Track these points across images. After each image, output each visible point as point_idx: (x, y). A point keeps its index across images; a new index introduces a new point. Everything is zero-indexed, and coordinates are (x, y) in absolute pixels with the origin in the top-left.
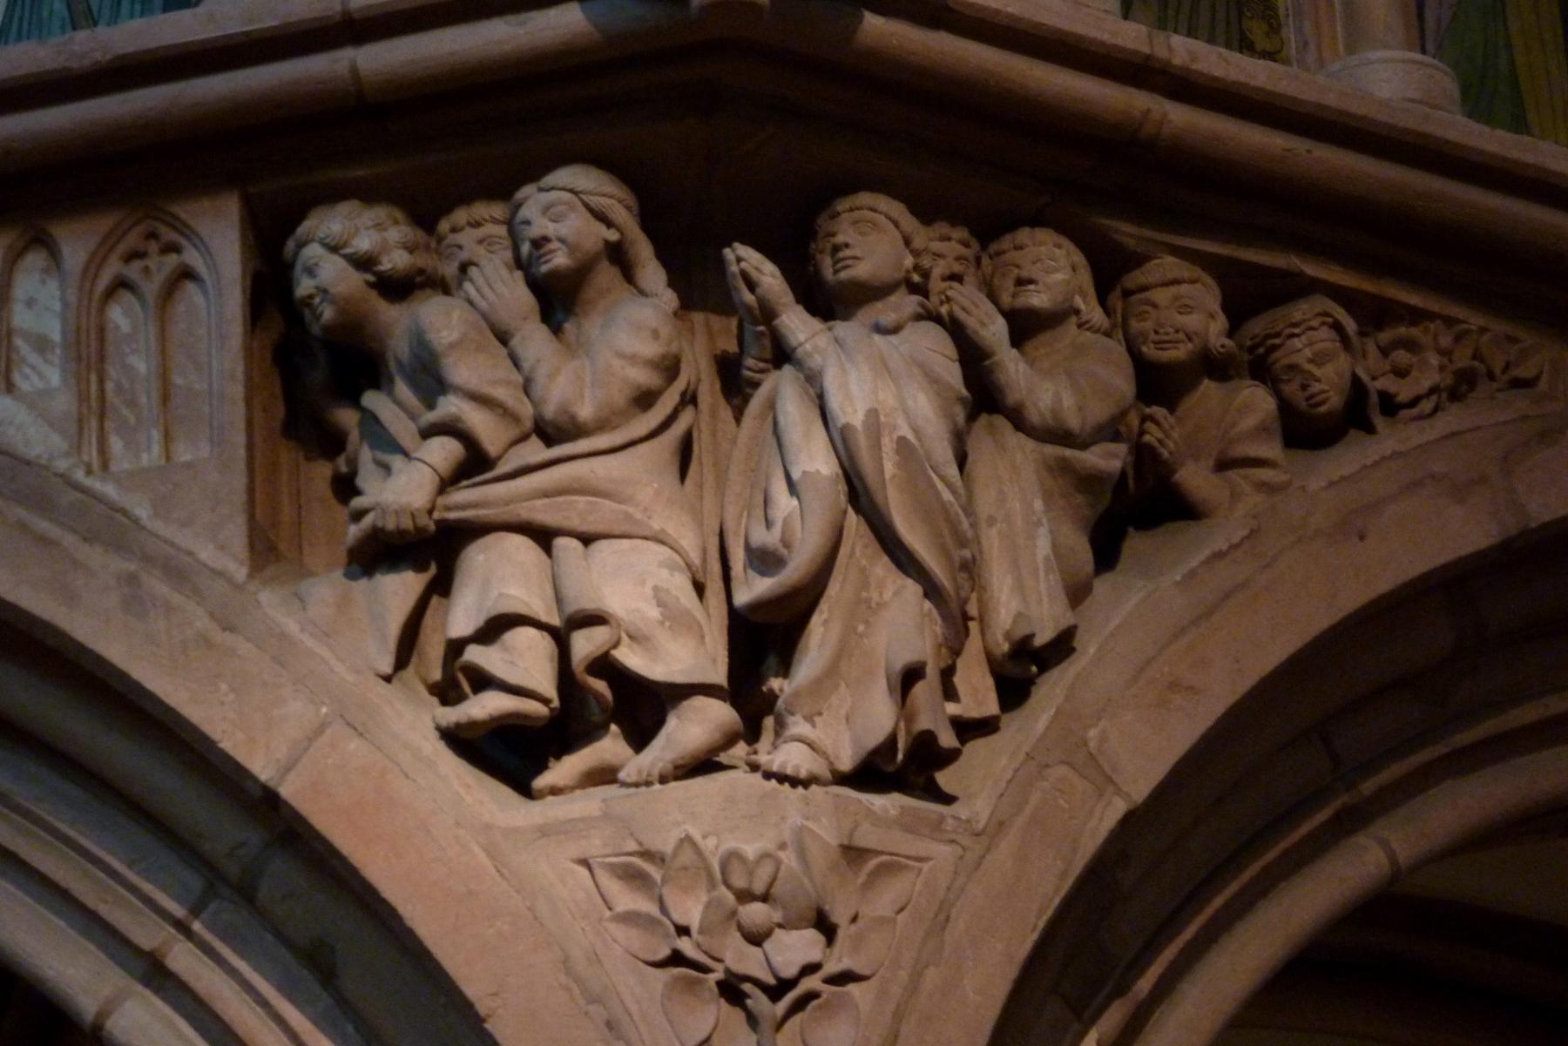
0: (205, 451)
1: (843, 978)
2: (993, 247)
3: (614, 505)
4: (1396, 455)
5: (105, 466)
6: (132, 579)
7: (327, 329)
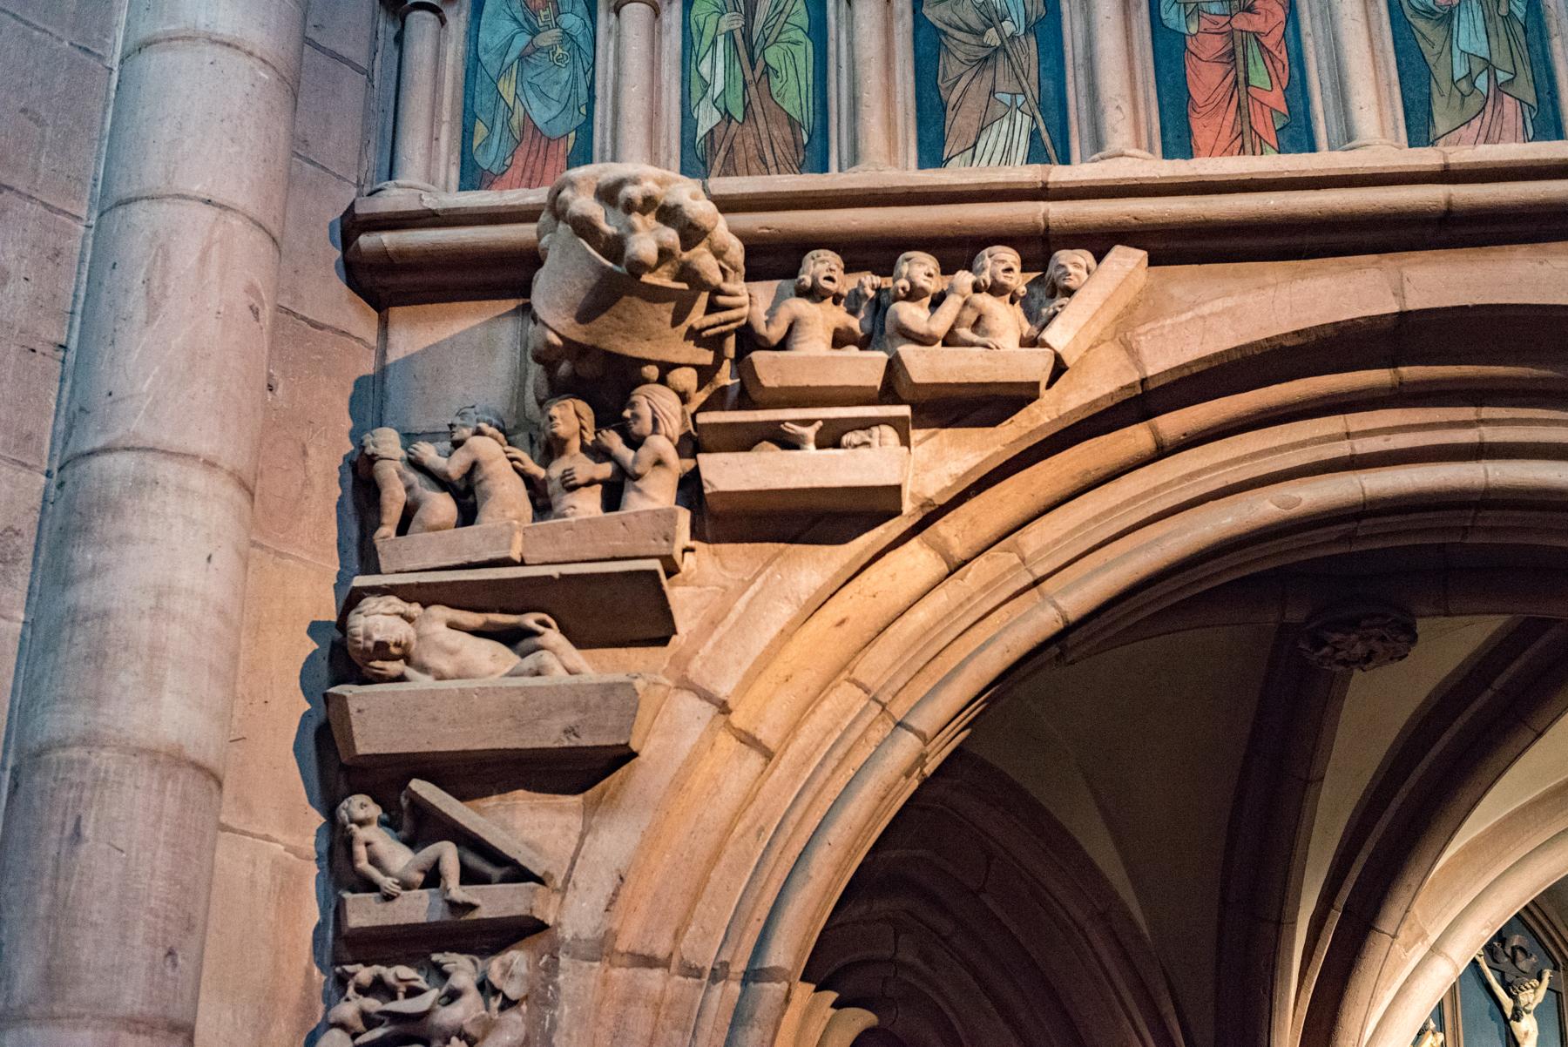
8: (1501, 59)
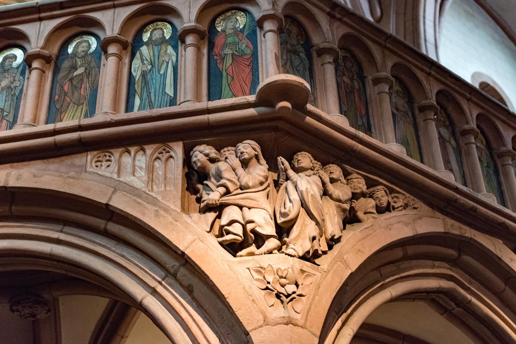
0: (173, 188)
1: (300, 295)
2: (325, 167)
3: (255, 202)
4: (395, 216)
5: (152, 191)
6: (157, 211)
7: (198, 168)
8: (7, 108)
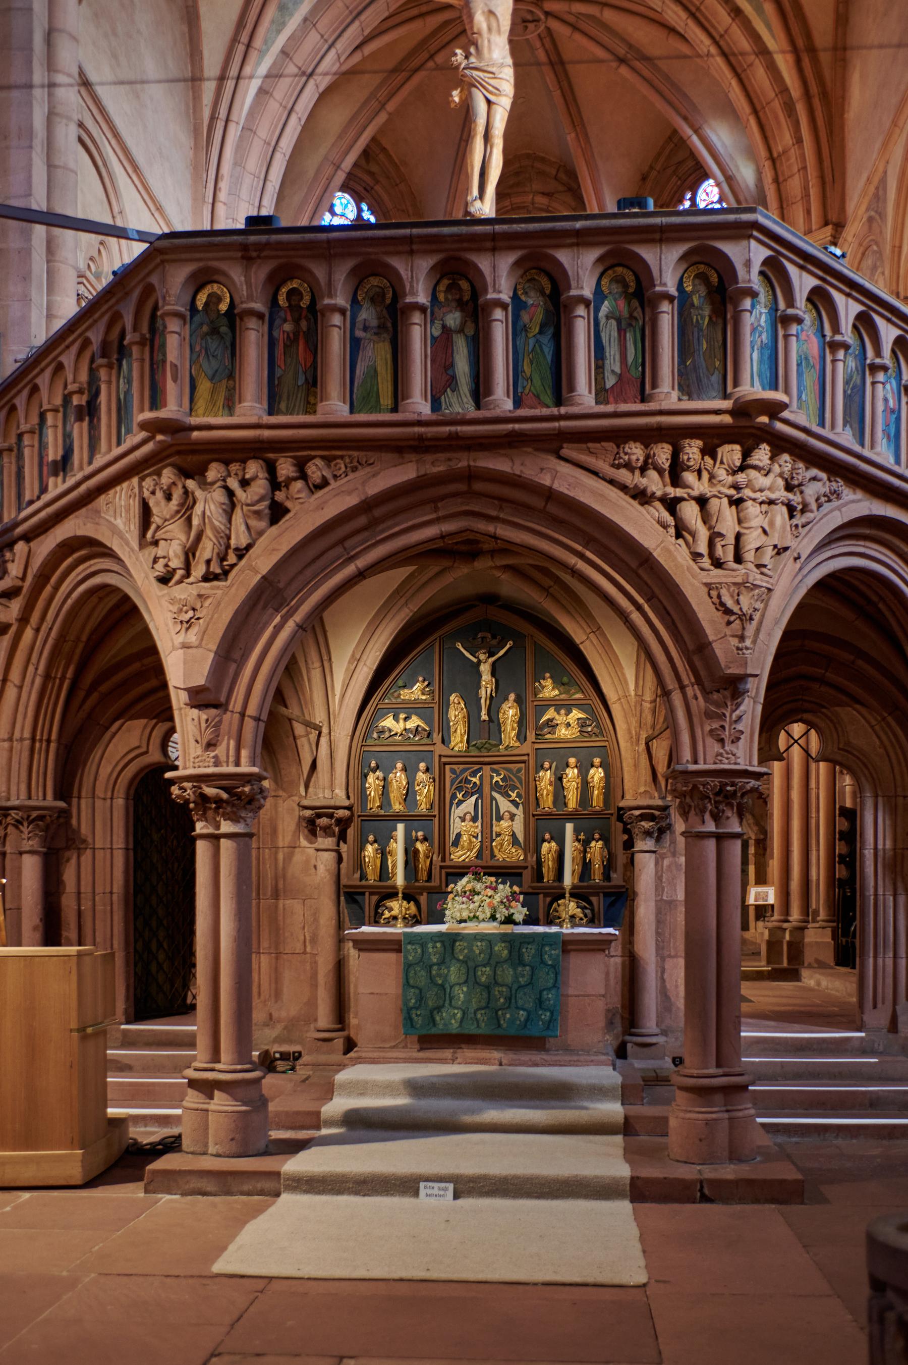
1: (198, 619)
